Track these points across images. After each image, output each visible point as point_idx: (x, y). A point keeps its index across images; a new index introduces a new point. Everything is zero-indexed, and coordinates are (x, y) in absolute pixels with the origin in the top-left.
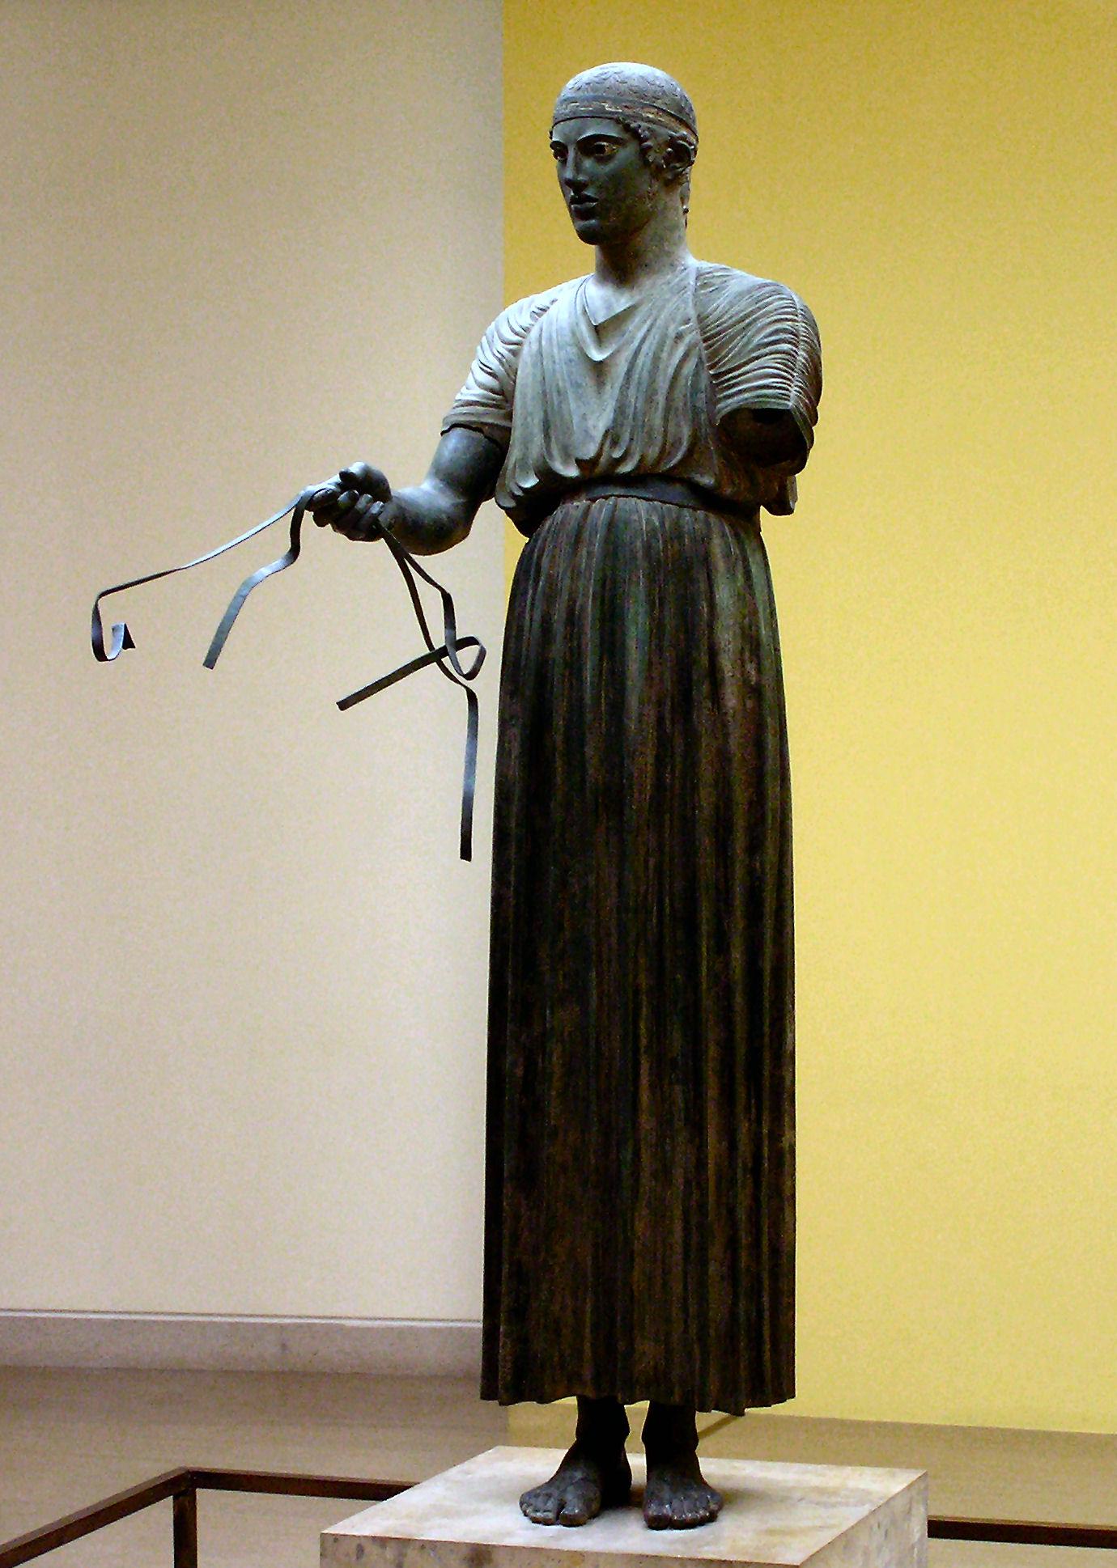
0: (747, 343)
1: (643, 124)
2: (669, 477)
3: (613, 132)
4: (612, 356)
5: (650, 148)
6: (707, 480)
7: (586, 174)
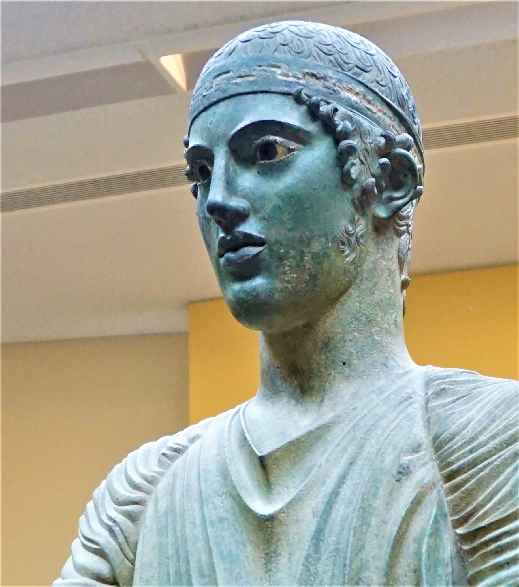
1: (342, 110)
3: (293, 116)
4: (290, 505)
5: (351, 150)
7: (245, 197)
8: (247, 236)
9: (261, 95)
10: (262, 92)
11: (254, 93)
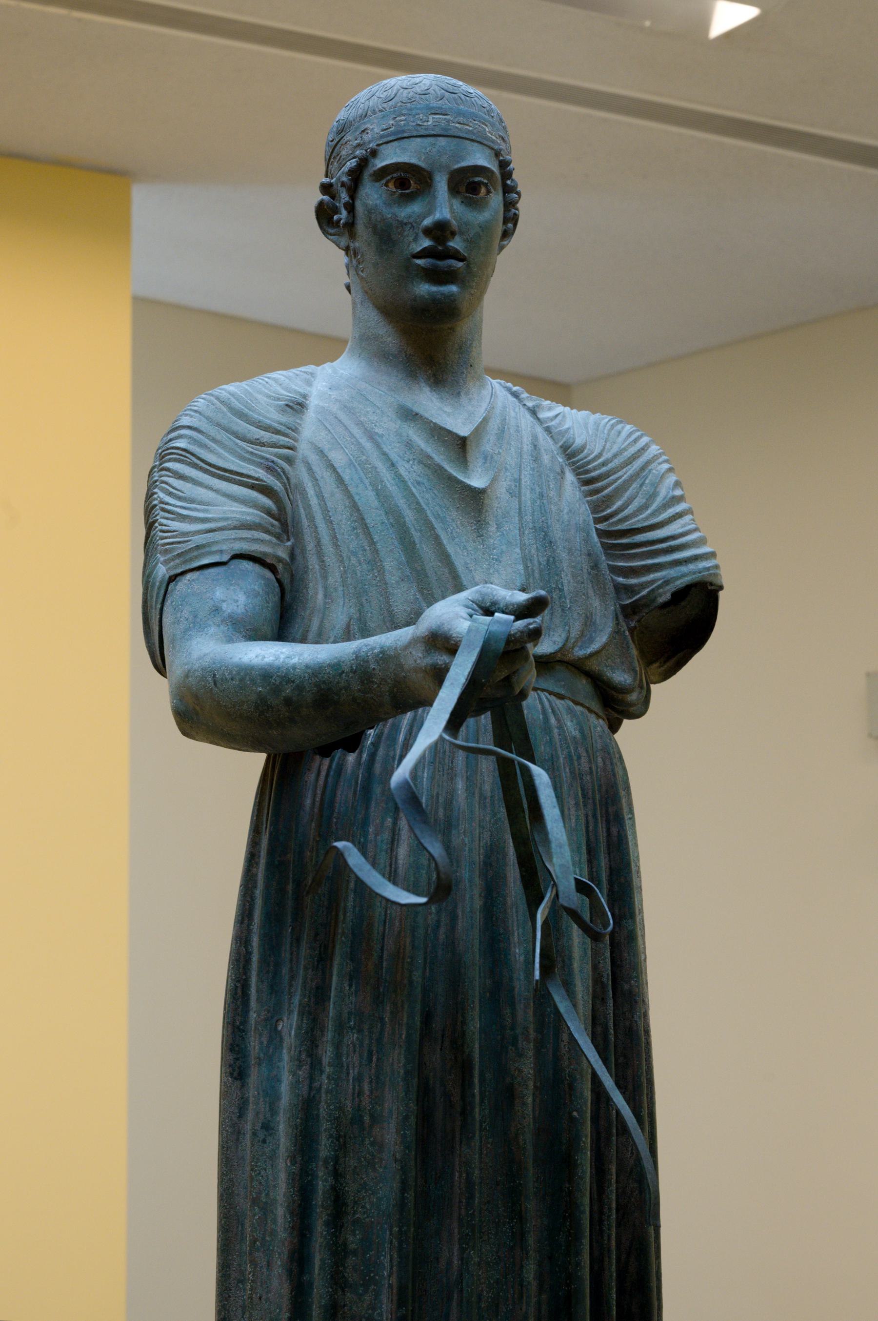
0: (653, 496)
2: (579, 667)
6: (620, 677)
8: (457, 251)
9: (476, 144)
10: (478, 142)
11: (472, 140)
